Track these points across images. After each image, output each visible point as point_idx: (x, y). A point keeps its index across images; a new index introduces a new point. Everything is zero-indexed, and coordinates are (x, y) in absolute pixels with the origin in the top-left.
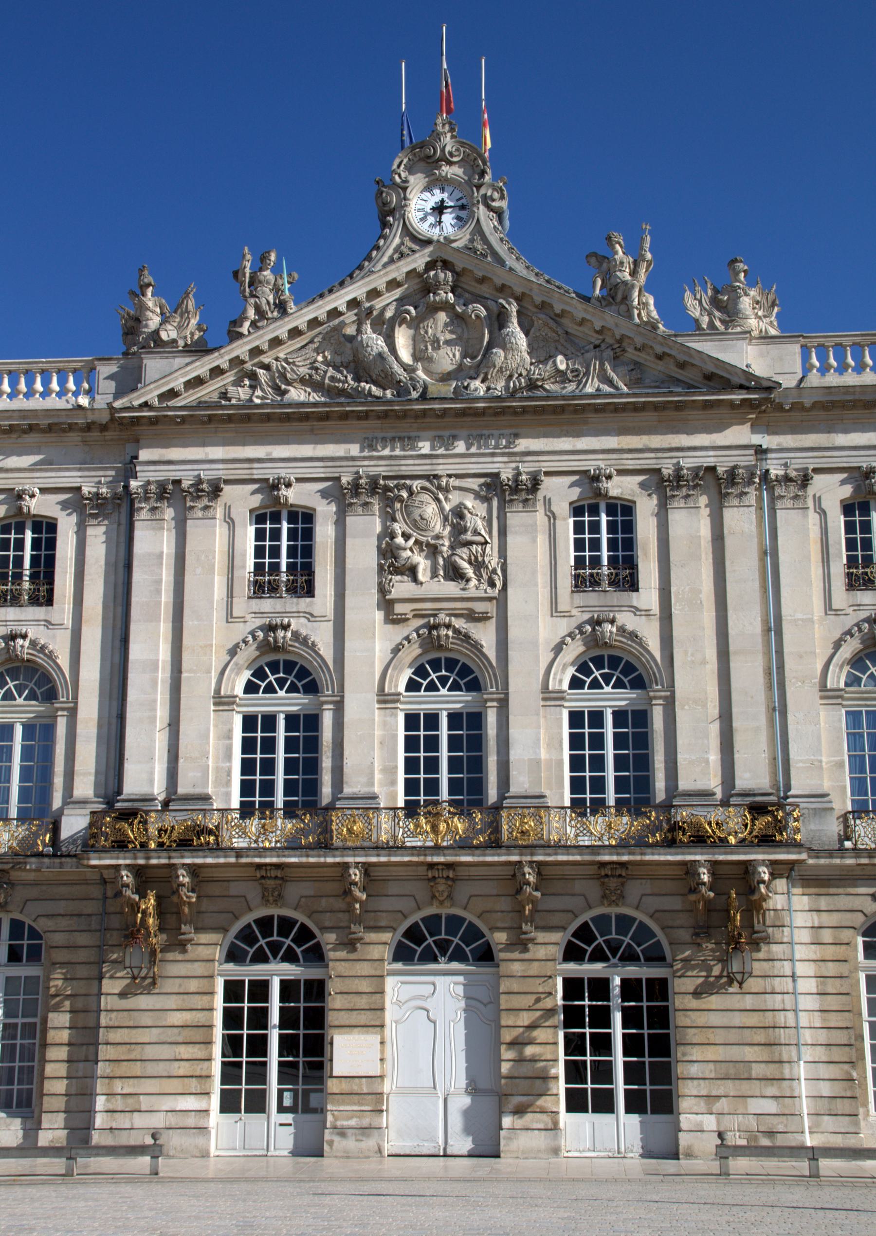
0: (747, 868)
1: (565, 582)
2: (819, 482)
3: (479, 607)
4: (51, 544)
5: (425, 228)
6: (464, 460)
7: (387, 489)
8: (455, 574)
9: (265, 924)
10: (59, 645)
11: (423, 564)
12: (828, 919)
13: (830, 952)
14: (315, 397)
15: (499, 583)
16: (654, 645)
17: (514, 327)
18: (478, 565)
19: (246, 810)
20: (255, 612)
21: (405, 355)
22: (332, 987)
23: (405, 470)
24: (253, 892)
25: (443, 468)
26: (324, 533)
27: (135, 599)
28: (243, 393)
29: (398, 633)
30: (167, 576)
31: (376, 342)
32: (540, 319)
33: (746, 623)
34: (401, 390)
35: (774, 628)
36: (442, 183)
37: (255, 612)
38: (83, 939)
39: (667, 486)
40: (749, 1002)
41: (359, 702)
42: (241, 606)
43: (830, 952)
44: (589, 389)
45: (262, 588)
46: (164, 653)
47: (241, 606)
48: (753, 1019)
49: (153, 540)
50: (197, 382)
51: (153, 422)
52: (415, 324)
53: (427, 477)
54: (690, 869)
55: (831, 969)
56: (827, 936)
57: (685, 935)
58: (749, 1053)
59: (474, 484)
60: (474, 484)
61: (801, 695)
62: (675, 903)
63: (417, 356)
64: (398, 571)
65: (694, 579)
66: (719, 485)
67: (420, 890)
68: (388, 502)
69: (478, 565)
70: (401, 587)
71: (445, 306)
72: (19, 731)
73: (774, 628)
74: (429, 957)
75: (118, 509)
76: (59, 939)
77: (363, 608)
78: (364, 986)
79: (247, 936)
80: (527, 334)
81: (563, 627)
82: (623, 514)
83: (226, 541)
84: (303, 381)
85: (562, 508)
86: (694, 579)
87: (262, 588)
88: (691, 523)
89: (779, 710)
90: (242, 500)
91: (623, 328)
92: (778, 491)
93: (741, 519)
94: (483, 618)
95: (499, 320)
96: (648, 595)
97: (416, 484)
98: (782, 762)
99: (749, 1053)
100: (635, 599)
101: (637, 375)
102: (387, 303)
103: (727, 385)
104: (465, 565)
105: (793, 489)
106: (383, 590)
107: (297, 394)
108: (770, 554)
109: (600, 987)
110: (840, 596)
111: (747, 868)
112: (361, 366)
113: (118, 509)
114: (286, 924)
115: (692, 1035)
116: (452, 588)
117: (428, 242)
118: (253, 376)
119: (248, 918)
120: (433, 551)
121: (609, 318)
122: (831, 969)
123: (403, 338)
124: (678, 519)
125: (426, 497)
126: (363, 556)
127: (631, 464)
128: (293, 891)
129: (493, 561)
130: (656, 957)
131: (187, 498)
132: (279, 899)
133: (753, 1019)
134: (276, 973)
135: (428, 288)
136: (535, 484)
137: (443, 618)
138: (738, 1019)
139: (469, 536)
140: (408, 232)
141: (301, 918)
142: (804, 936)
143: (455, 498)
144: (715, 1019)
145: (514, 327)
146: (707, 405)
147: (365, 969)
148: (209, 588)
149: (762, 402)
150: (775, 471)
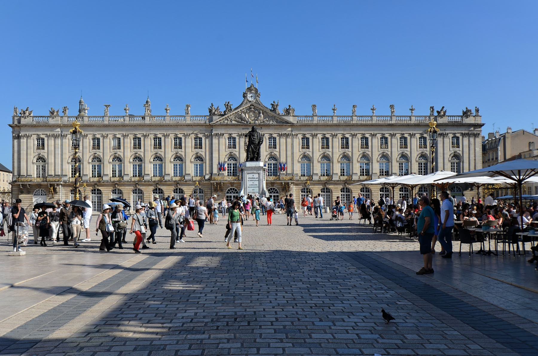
0: (288, 183)
1: (268, 147)
2: (299, 135)
4: (201, 141)
5: (250, 99)
9: (231, 189)
10: (203, 154)
16: (278, 156)
17: (261, 114)
20: (229, 151)
21: (247, 117)
24: (230, 185)
26: (237, 140)
28: (226, 121)
30: (217, 145)
31: (243, 115)
33: (289, 153)
34: (247, 122)
35: (293, 154)
36: (252, 93)
37: (229, 151)
39: (280, 136)
42: (227, 150)
45: (229, 148)
46: (217, 156)
47: (227, 150)
49: (215, 141)
52: (248, 114)
61: (295, 162)
65: (283, 147)
66: (287, 136)
73: (293, 154)
75: (210, 137)
79: (229, 190)
81: (267, 153)
82: (275, 139)
85: (267, 138)
86: (283, 147)
87: (229, 148)
88: (283, 140)
89: (293, 164)
90: (226, 136)
91: (275, 115)
93: (289, 140)
95: (260, 113)
96: (277, 149)
98: (293, 170)
100: (276, 150)
102: (245, 110)
103: (288, 123)
107: (233, 122)
108: (292, 144)
110: (301, 150)
111: (288, 183)
113: (210, 137)
114: (234, 189)
117: (250, 102)
121: (273, 114)
123: (247, 115)
124: (281, 140)
128: (235, 185)
130: (277, 193)
131: (219, 136)
134: (232, 195)
135: (250, 108)
140: (248, 100)
145: (261, 114)
148: (222, 147)
149: (292, 125)
150: (294, 134)
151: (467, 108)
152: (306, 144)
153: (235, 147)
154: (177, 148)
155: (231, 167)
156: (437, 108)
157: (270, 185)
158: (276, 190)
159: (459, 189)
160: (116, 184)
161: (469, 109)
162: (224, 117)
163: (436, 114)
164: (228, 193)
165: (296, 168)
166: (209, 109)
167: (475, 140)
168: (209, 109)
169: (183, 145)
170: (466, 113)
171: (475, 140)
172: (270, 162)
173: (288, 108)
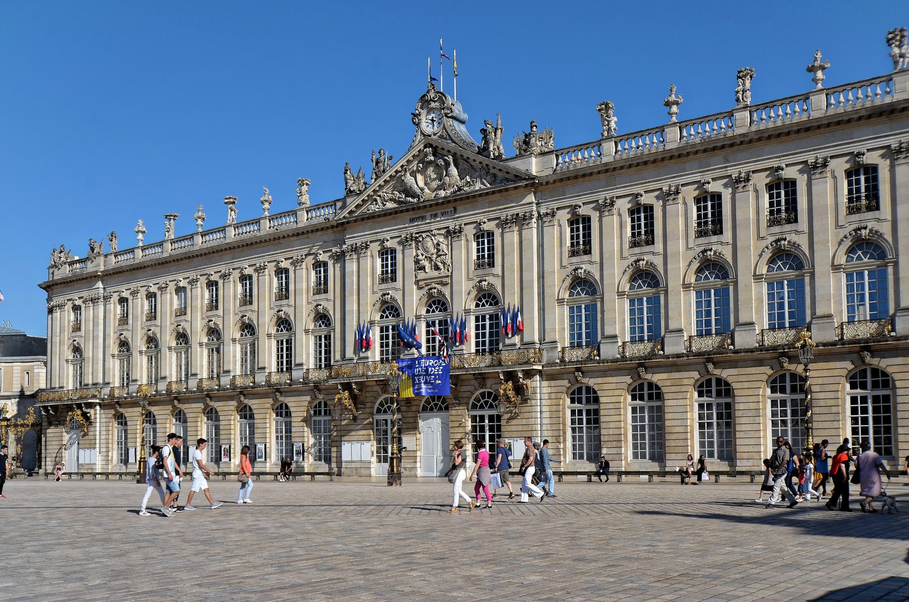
3: (444, 280)
6: (438, 224)
7: (417, 238)
8: (437, 268)
9: (386, 401)
11: (426, 264)
12: (554, 390)
13: (554, 402)
14: (395, 205)
18: (444, 263)
21: (421, 183)
22: (602, 412)
23: (422, 229)
26: (399, 256)
27: (347, 289)
30: (355, 279)
32: (461, 162)
39: (503, 224)
40: (524, 422)
43: (554, 402)
44: (477, 188)
48: (525, 428)
49: (351, 266)
50: (358, 206)
53: (428, 231)
55: (554, 408)
56: (553, 396)
59: (443, 232)
60: (443, 232)
63: (426, 184)
64: (420, 269)
68: (417, 242)
69: (444, 263)
70: (421, 275)
71: (431, 162)
73: (541, 276)
74: (432, 409)
78: (411, 420)
79: (381, 404)
80: (457, 169)
83: (373, 264)
84: (391, 200)
85: (471, 237)
88: (513, 236)
92: (545, 219)
94: (445, 284)
95: (447, 164)
97: (424, 235)
101: (494, 179)
104: (439, 264)
105: (549, 218)
107: (390, 205)
112: (408, 192)
113: (340, 258)
115: (506, 434)
116: (435, 274)
118: (376, 200)
120: (431, 260)
122: (554, 408)
123: (420, 177)
125: (428, 239)
126: (410, 265)
127: (492, 216)
129: (449, 262)
133: (525, 428)
137: (434, 285)
138: (520, 428)
139: (441, 253)
140: (422, 133)
142: (546, 396)
144: (513, 428)
146: (516, 188)
147: (410, 414)
149: (533, 184)
160: (783, 354)
164: (379, 411)
165: (550, 325)
172: (482, 311)
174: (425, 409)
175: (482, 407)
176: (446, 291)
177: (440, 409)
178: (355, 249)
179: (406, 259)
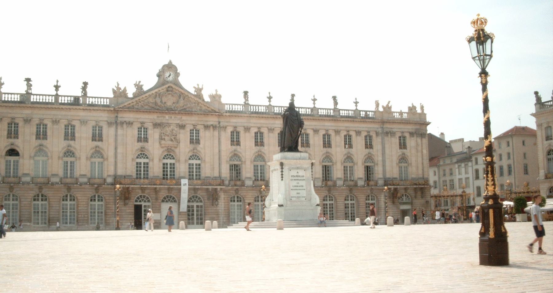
0: (216, 189)
11: (166, 138)
15: (178, 142)
19: (137, 178)
24: (140, 191)
25: (170, 122)
29: (163, 150)
38: (111, 198)
40: (215, 208)
41: (156, 161)
51: (121, 111)
54: (207, 189)
57: (206, 199)
58: (214, 216)
62: (205, 194)
67: (167, 191)
70: (163, 142)
72: (97, 163)
74: (167, 202)
76: (107, 198)
77: (157, 145)
79: (138, 198)
83: (132, 133)
99: (214, 216)
106: (160, 143)
109: (193, 207)
114: (144, 197)
116: (170, 142)
119: (138, 195)
126: (157, 136)
128: (147, 191)
130: (201, 201)
132: (144, 193)
136: (185, 126)
137: (169, 148)
141: (147, 196)
143: (172, 127)
144: (210, 211)
147: (157, 204)
151: (412, 104)
152: (235, 140)
153: (146, 140)
154: (68, 140)
155: (140, 167)
156: (383, 103)
157: (193, 192)
158: (199, 198)
159: (408, 196)
161: (414, 105)
162: (134, 101)
163: (381, 109)
164: (136, 201)
166: (113, 89)
167: (422, 140)
168: (113, 89)
169: (76, 135)
170: (412, 109)
171: (422, 140)
173: (214, 93)
174: (163, 201)
175: (193, 202)
176: (177, 151)
177: (172, 202)
178: (122, 123)
179: (154, 135)
